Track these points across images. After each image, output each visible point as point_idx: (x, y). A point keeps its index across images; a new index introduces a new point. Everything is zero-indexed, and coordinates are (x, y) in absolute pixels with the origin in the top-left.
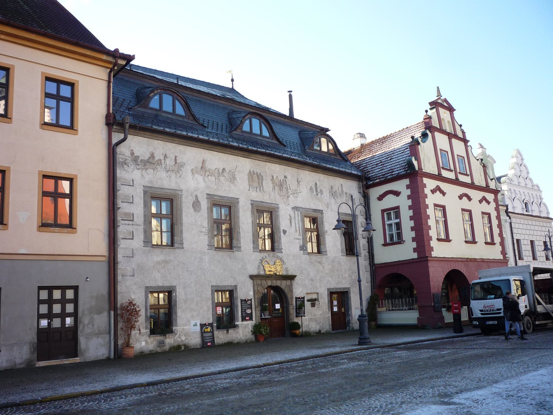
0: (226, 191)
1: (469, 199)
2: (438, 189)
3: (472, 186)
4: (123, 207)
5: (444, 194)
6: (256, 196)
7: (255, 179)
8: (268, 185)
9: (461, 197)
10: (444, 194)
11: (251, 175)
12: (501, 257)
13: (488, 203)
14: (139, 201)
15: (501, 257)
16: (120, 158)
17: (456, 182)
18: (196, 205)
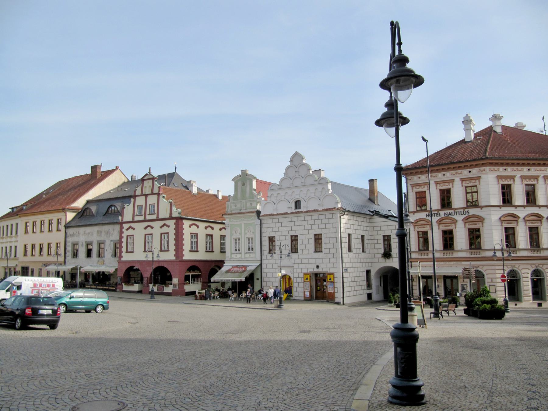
0: (90, 239)
1: (152, 228)
2: (130, 227)
3: (158, 220)
4: (67, 248)
5: (134, 229)
6: (99, 239)
7: (99, 232)
8: (103, 234)
9: (146, 228)
10: (134, 229)
11: (98, 232)
12: (174, 258)
13: (169, 226)
14: (71, 246)
15: (174, 258)
16: (67, 235)
17: (145, 221)
18: (82, 245)
